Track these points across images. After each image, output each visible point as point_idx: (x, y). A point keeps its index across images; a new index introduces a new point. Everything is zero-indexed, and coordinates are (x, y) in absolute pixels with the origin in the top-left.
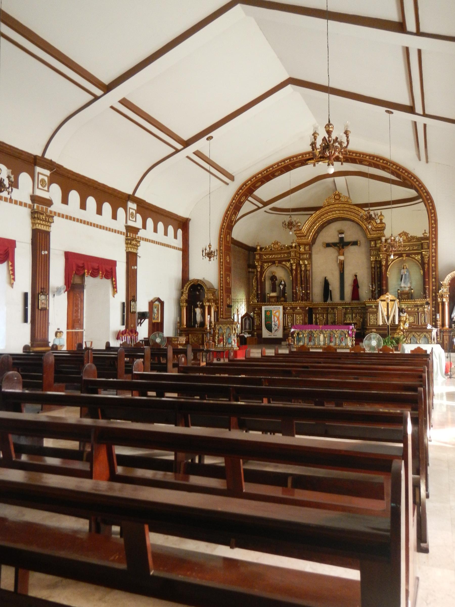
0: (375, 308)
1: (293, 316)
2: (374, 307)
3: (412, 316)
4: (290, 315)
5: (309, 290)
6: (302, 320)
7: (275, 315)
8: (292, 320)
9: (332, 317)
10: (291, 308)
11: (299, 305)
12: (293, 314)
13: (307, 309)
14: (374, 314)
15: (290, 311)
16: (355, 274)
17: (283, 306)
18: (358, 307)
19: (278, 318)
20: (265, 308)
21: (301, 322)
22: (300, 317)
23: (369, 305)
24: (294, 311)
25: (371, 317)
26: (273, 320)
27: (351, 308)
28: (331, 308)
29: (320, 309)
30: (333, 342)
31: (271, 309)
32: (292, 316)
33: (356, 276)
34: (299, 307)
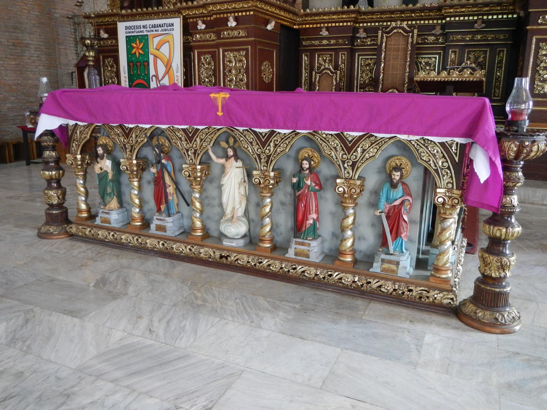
1: (215, 57)
4: (208, 53)
6: (247, 72)
7: (156, 52)
8: (214, 71)
9: (369, 65)
10: (210, 25)
11: (234, 12)
13: (270, 27)
15: (208, 36)
17: (185, 19)
18: (476, 21)
19: (168, 66)
20: (127, 28)
21: (242, 80)
22: (241, 61)
26: (152, 72)
27: (443, 27)
28: (366, 30)
29: (325, 33)
30: (314, 233)
31: (145, 33)
34: (236, 19)
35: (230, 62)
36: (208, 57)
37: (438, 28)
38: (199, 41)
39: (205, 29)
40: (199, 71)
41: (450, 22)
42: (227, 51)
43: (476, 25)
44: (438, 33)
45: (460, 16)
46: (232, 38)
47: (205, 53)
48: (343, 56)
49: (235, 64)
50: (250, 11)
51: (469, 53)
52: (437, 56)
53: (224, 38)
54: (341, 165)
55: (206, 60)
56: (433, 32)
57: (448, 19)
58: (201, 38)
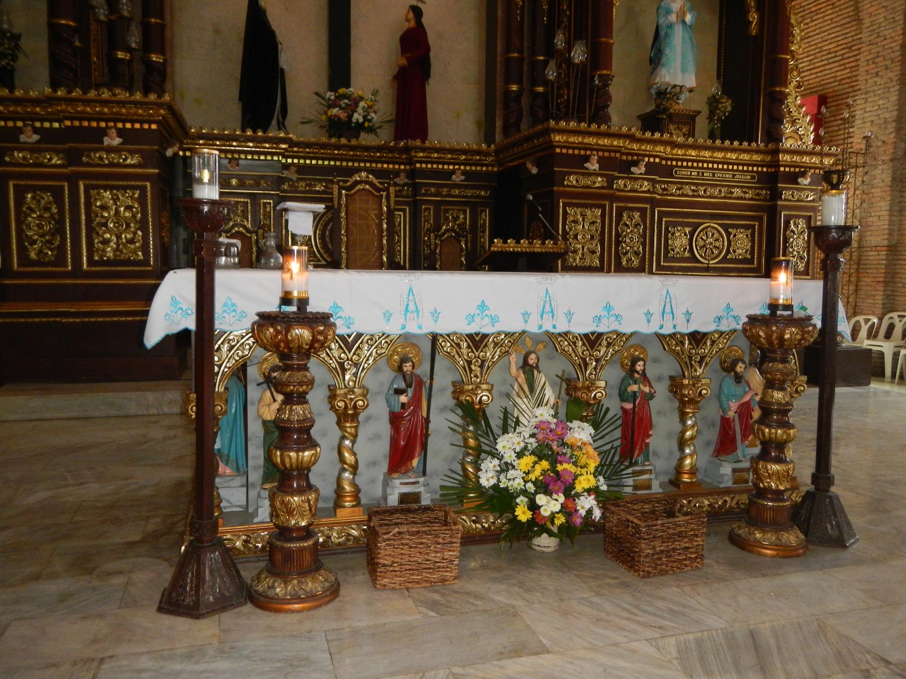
0: (602, 175)
2: (593, 166)
3: (746, 227)
4: (45, 189)
5: (162, 52)
11: (115, 121)
12: (73, 180)
14: (591, 206)
16: (414, 3)
18: (453, 172)
21: (131, 241)
23: (567, 154)
24: (73, 158)
25: (575, 222)
32: (57, 194)
33: (417, 12)
34: (121, 133)
35: (104, 208)
36: (47, 197)
37: (403, 175)
38: (21, 165)
39: (37, 142)
40: (19, 222)
41: (421, 170)
42: (98, 187)
43: (454, 176)
44: (402, 183)
45: (432, 163)
46: (112, 165)
47: (33, 189)
48: (268, 206)
49: (117, 212)
50: (150, 122)
51: (447, 211)
52: (401, 213)
53: (88, 165)
54: (688, 362)
55: (39, 201)
56: (397, 180)
57: (418, 165)
58: (24, 158)
